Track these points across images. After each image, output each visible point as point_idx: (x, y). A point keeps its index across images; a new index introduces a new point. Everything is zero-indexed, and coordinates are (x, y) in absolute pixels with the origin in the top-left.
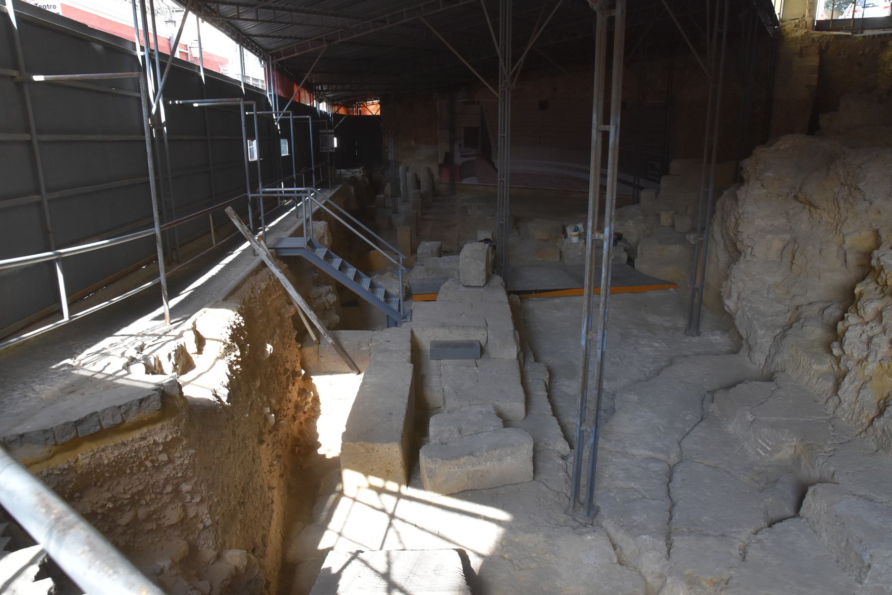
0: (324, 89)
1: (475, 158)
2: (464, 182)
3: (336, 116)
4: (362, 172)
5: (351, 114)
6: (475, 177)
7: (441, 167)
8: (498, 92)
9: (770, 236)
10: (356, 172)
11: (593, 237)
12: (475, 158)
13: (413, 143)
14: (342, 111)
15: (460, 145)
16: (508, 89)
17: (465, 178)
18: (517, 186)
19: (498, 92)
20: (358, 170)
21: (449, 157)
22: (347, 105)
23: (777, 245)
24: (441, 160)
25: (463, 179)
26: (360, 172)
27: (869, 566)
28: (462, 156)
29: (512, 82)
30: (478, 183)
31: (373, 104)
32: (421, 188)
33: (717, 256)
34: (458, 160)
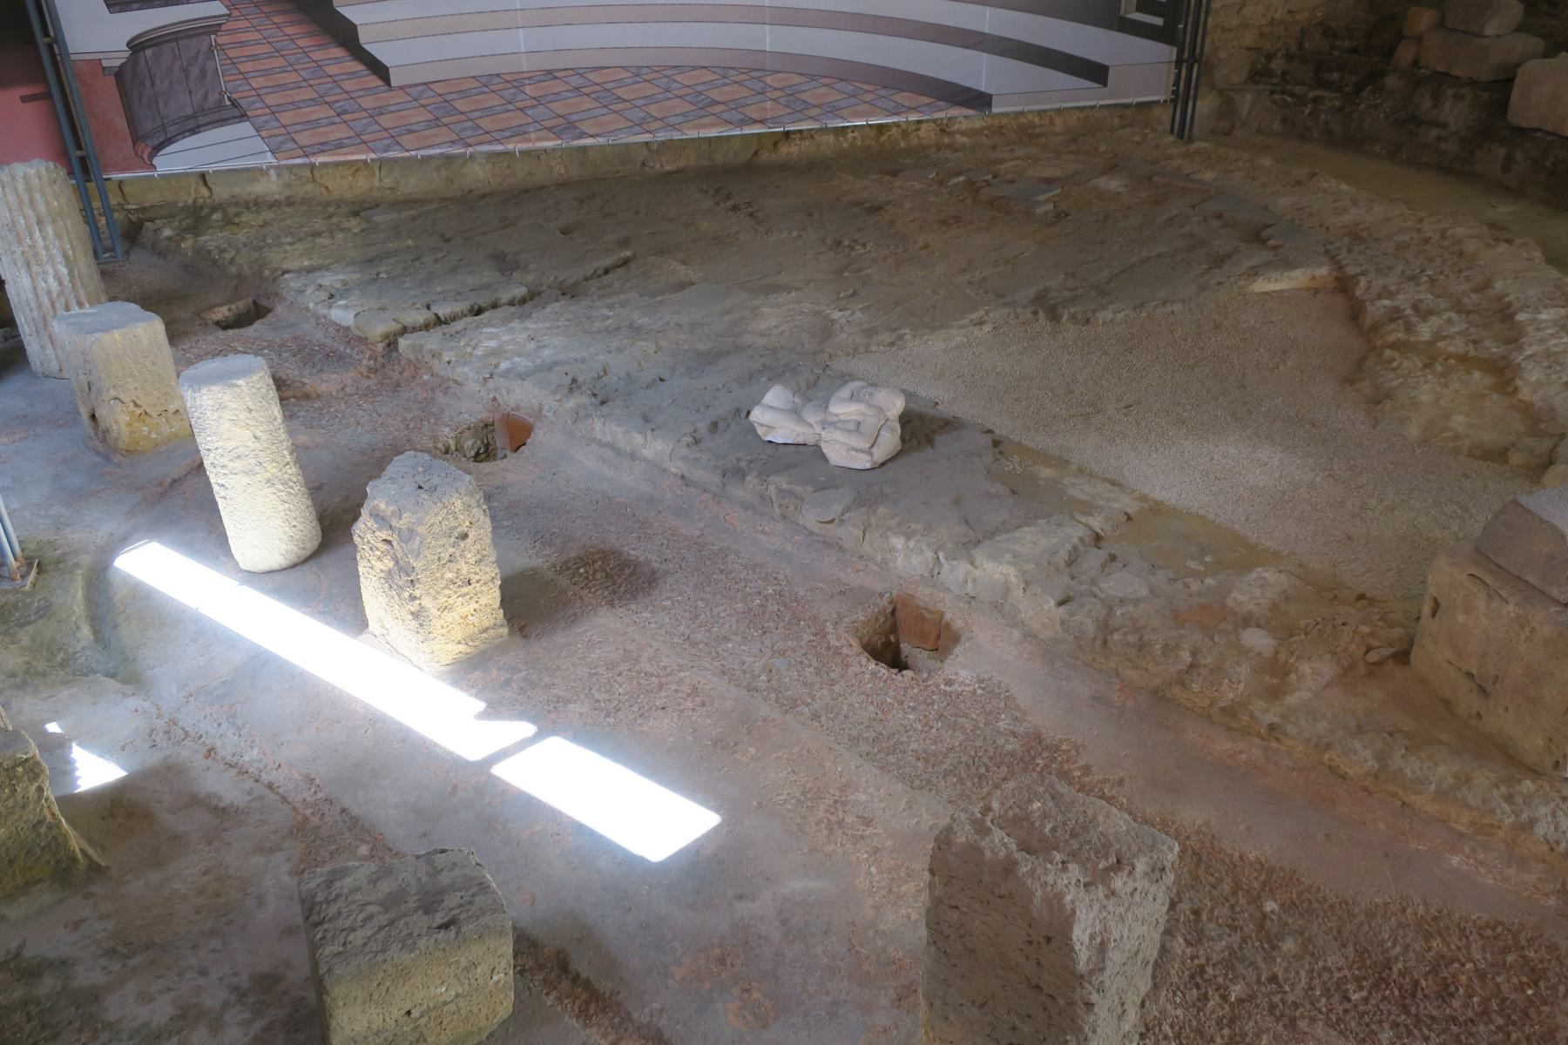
6: (245, 128)
17: (169, 141)
25: (157, 149)
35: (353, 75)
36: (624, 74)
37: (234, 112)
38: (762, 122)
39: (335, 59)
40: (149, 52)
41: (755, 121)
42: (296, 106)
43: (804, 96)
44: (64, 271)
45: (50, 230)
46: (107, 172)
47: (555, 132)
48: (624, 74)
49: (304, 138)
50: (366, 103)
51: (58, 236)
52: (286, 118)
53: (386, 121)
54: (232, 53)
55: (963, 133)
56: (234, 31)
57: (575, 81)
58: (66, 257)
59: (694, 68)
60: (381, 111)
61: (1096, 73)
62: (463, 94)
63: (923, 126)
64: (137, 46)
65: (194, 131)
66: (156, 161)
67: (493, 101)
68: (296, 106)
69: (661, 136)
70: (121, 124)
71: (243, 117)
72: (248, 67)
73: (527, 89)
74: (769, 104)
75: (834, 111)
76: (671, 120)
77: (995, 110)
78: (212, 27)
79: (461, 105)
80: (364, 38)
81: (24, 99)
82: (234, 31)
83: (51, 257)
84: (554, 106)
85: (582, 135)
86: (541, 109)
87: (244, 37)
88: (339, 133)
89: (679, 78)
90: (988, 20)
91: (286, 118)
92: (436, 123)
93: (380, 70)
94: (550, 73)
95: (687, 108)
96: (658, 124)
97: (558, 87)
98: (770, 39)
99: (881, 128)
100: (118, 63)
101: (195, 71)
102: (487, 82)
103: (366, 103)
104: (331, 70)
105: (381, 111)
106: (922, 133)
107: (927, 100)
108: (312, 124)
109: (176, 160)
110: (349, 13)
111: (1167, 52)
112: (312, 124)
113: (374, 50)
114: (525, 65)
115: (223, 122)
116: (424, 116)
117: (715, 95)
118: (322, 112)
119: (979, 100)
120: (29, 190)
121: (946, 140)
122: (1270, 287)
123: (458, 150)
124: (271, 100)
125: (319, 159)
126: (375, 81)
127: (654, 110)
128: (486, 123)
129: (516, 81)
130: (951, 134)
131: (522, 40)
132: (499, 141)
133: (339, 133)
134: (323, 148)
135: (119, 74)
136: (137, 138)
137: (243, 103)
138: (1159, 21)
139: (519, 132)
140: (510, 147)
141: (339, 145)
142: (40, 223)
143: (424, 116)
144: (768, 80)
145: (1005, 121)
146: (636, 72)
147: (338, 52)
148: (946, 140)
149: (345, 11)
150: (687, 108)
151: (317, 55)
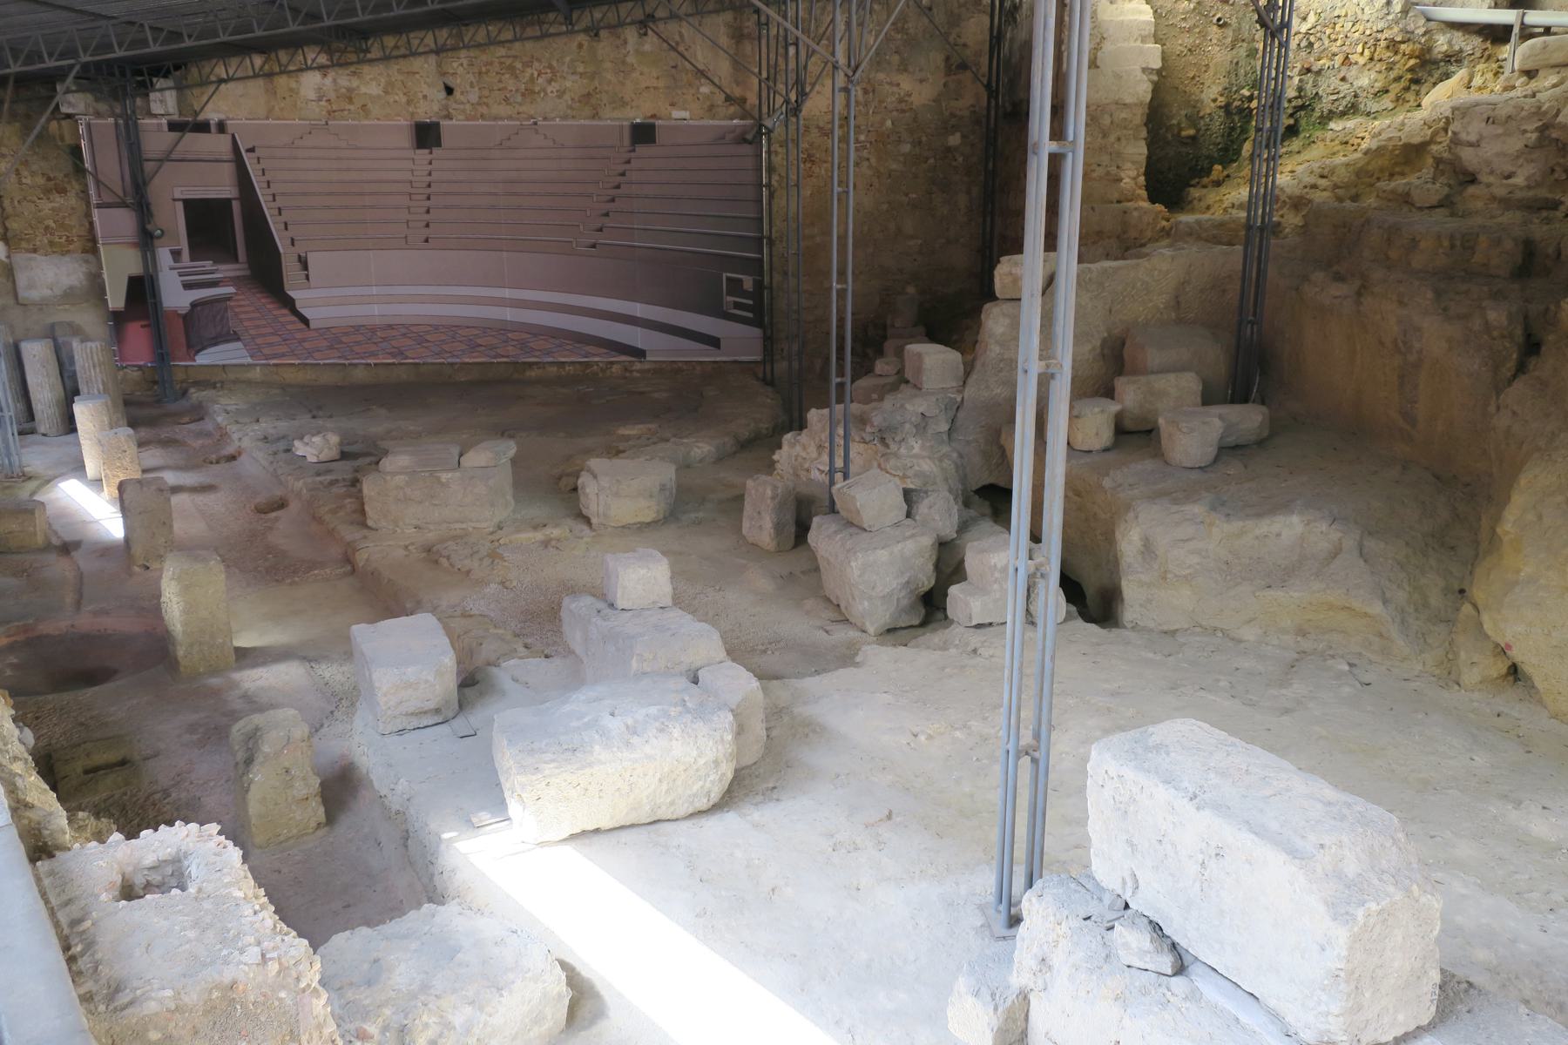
1: (231, 290)
6: (239, 345)
7: (118, 320)
12: (231, 290)
15: (176, 255)
21: (142, 290)
24: (116, 299)
25: (198, 352)
28: (188, 286)
30: (249, 360)
33: (1177, 512)
34: (175, 296)
35: (293, 323)
36: (429, 328)
38: (508, 357)
39: (284, 315)
40: (199, 308)
41: (503, 356)
42: (263, 335)
43: (531, 345)
44: (101, 387)
45: (98, 370)
46: (174, 361)
47: (393, 355)
48: (429, 328)
49: (267, 351)
50: (298, 336)
51: (101, 372)
52: (259, 341)
53: (306, 345)
54: (237, 310)
55: (638, 371)
56: (238, 300)
57: (403, 331)
58: (103, 381)
59: (468, 327)
60: (304, 340)
61: (714, 342)
62: (346, 334)
63: (615, 366)
64: (194, 305)
65: (216, 344)
66: (196, 358)
67: (360, 338)
68: (263, 335)
69: (450, 360)
70: (183, 340)
71: (238, 339)
72: (243, 316)
73: (379, 334)
74: (510, 348)
75: (548, 354)
76: (455, 353)
77: (648, 359)
78: (228, 298)
79: (344, 339)
80: (298, 305)
81: (142, 326)
82: (238, 300)
83: (97, 380)
84: (393, 342)
85: (407, 358)
86: (385, 344)
87: (243, 303)
88: (284, 349)
89: (460, 332)
90: (638, 309)
91: (259, 341)
92: (331, 347)
93: (305, 321)
94: (390, 327)
95: (464, 347)
96: (449, 355)
97: (393, 333)
98: (509, 314)
99: (588, 365)
100: (184, 312)
101: (219, 317)
102: (357, 329)
103: (298, 336)
104: (281, 319)
105: (304, 340)
106: (613, 370)
107: (606, 351)
108: (271, 345)
109: (203, 359)
110: (292, 293)
111: (757, 332)
112: (271, 345)
113: (304, 311)
114: (377, 321)
115: (227, 341)
116: (325, 343)
117: (479, 341)
118: (276, 339)
119: (640, 353)
120: (91, 352)
121: (628, 374)
122: (627, 432)
124: (252, 332)
126: (303, 326)
127: (446, 347)
128: (357, 349)
129: (373, 329)
130: (631, 372)
131: (376, 310)
132: (363, 358)
133: (284, 349)
134: (275, 356)
135: (185, 317)
136: (189, 346)
137: (239, 333)
138: (750, 315)
139: (373, 354)
140: (369, 361)
141: (283, 355)
142: (94, 366)
143: (325, 343)
144: (509, 335)
145: (664, 366)
146: (436, 327)
147: (285, 311)
148: (628, 374)
149: (290, 293)
150: (464, 347)
151: (275, 313)
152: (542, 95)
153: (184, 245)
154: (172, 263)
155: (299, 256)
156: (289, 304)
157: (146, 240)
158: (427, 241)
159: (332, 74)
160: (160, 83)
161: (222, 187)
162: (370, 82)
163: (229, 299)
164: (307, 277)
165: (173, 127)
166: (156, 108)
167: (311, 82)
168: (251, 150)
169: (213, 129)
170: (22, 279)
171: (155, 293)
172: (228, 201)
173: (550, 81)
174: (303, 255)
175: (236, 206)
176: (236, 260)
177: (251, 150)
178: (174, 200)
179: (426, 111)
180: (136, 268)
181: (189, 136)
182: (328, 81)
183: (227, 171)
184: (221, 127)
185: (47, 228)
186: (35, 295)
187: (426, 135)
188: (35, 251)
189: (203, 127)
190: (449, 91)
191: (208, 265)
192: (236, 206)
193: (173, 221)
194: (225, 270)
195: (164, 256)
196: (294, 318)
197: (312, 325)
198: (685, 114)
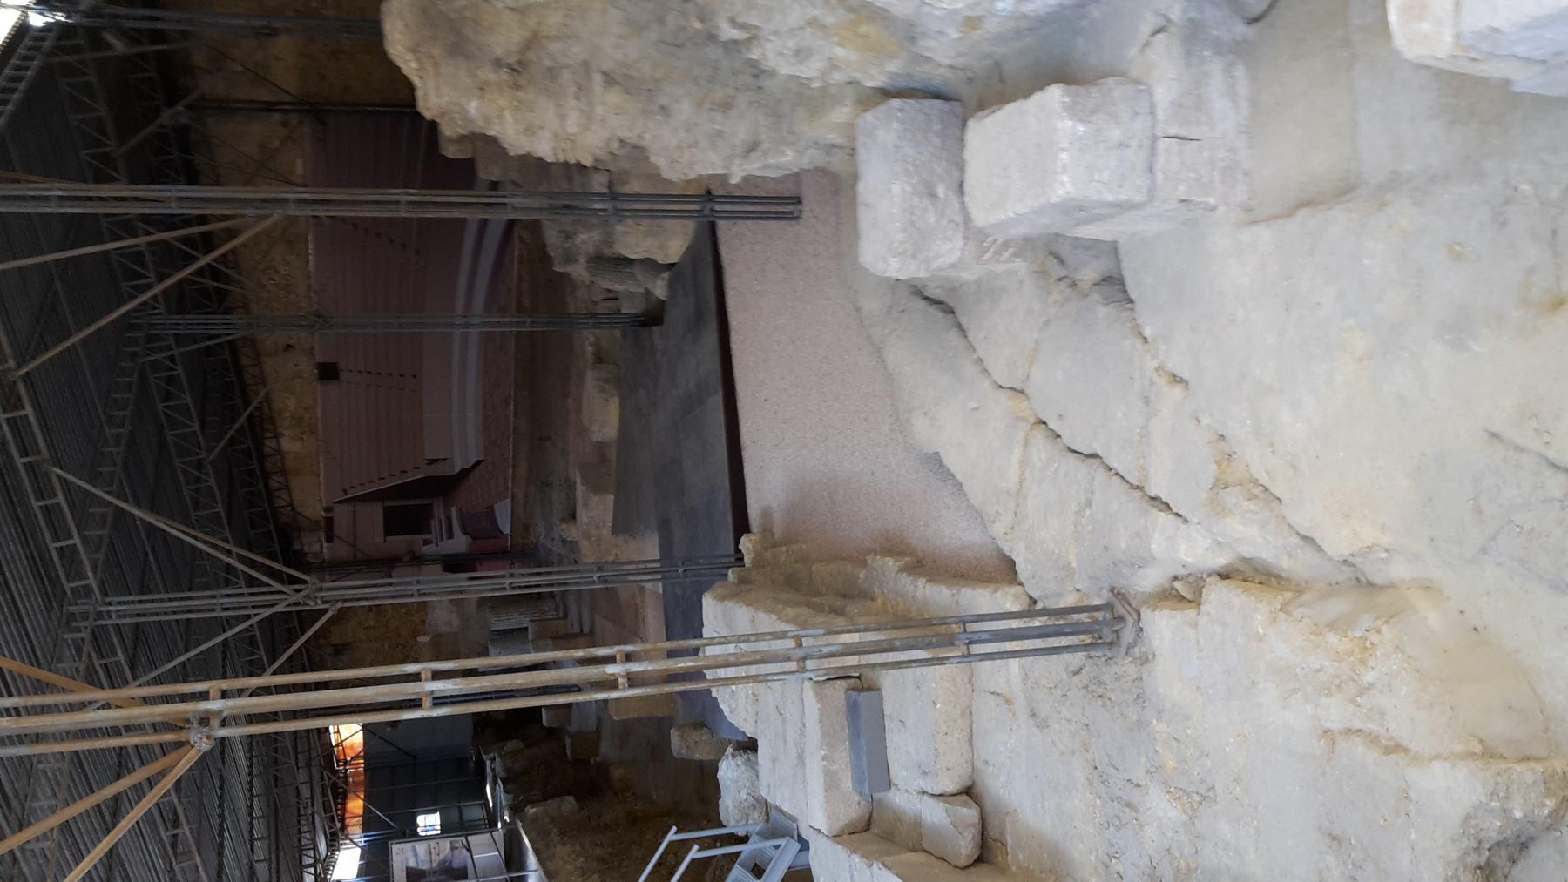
0: (311, 861)
2: (507, 530)
3: (368, 824)
4: (492, 755)
5: (362, 777)
6: (496, 507)
8: (327, 610)
9: (599, 110)
10: (493, 770)
11: (624, 688)
12: (454, 509)
13: (423, 639)
14: (356, 805)
15: (426, 542)
16: (321, 589)
17: (499, 529)
18: (512, 419)
19: (327, 610)
20: (488, 763)
22: (341, 796)
23: (614, 97)
25: (501, 532)
26: (493, 759)
27: (1183, 201)
28: (451, 536)
29: (305, 582)
30: (508, 500)
31: (338, 732)
32: (525, 625)
34: (459, 543)
37: (490, 511)
46: (507, 547)
64: (465, 533)
65: (496, 521)
71: (492, 507)
78: (460, 512)
93: (479, 463)
110: (457, 470)
113: (470, 465)
123: (511, 439)
125: (510, 484)
126: (483, 464)
131: (470, 414)
135: (474, 538)
147: (471, 475)
152: (289, 278)
153: (419, 538)
154: (433, 545)
155: (428, 464)
156: (465, 473)
157: (417, 560)
158: (414, 376)
159: (280, 430)
160: (297, 546)
161: (376, 511)
162: (287, 404)
163: (461, 510)
164: (444, 460)
165: (329, 539)
166: (316, 548)
167: (287, 444)
168: (345, 492)
169: (330, 515)
170: (443, 629)
171: (456, 556)
172: (384, 507)
173: (277, 271)
174: (426, 462)
175: (389, 503)
176: (432, 504)
177: (345, 492)
178: (385, 541)
179: (307, 368)
180: (439, 567)
181: (336, 531)
182: (286, 432)
183: (360, 507)
184: (328, 510)
185: (406, 613)
186: (456, 622)
187: (328, 372)
188: (423, 621)
189: (329, 522)
190: (289, 347)
191: (434, 523)
192: (389, 503)
193: (399, 543)
194: (439, 512)
195: (428, 549)
196: (476, 471)
197: (482, 458)
198: (299, 162)
